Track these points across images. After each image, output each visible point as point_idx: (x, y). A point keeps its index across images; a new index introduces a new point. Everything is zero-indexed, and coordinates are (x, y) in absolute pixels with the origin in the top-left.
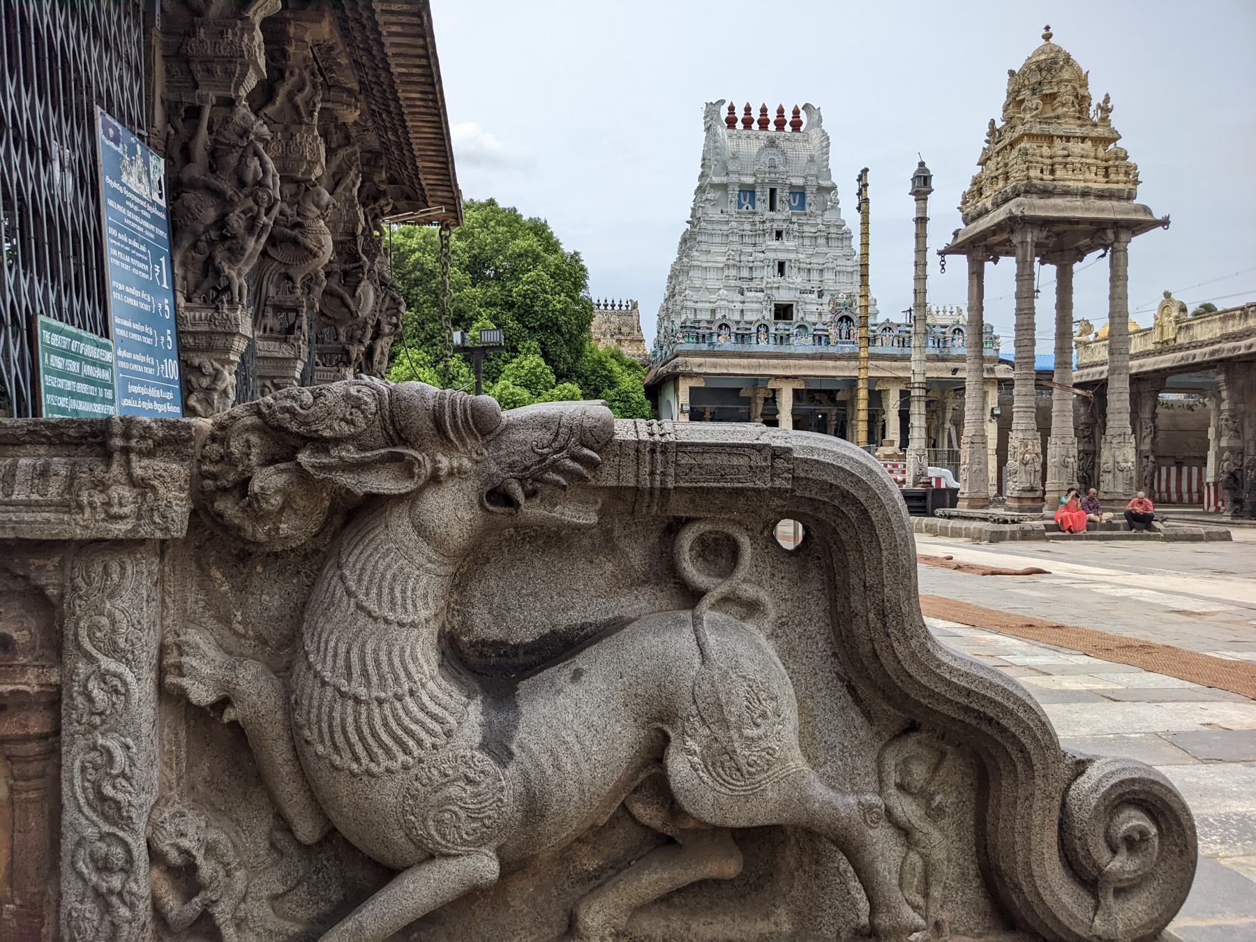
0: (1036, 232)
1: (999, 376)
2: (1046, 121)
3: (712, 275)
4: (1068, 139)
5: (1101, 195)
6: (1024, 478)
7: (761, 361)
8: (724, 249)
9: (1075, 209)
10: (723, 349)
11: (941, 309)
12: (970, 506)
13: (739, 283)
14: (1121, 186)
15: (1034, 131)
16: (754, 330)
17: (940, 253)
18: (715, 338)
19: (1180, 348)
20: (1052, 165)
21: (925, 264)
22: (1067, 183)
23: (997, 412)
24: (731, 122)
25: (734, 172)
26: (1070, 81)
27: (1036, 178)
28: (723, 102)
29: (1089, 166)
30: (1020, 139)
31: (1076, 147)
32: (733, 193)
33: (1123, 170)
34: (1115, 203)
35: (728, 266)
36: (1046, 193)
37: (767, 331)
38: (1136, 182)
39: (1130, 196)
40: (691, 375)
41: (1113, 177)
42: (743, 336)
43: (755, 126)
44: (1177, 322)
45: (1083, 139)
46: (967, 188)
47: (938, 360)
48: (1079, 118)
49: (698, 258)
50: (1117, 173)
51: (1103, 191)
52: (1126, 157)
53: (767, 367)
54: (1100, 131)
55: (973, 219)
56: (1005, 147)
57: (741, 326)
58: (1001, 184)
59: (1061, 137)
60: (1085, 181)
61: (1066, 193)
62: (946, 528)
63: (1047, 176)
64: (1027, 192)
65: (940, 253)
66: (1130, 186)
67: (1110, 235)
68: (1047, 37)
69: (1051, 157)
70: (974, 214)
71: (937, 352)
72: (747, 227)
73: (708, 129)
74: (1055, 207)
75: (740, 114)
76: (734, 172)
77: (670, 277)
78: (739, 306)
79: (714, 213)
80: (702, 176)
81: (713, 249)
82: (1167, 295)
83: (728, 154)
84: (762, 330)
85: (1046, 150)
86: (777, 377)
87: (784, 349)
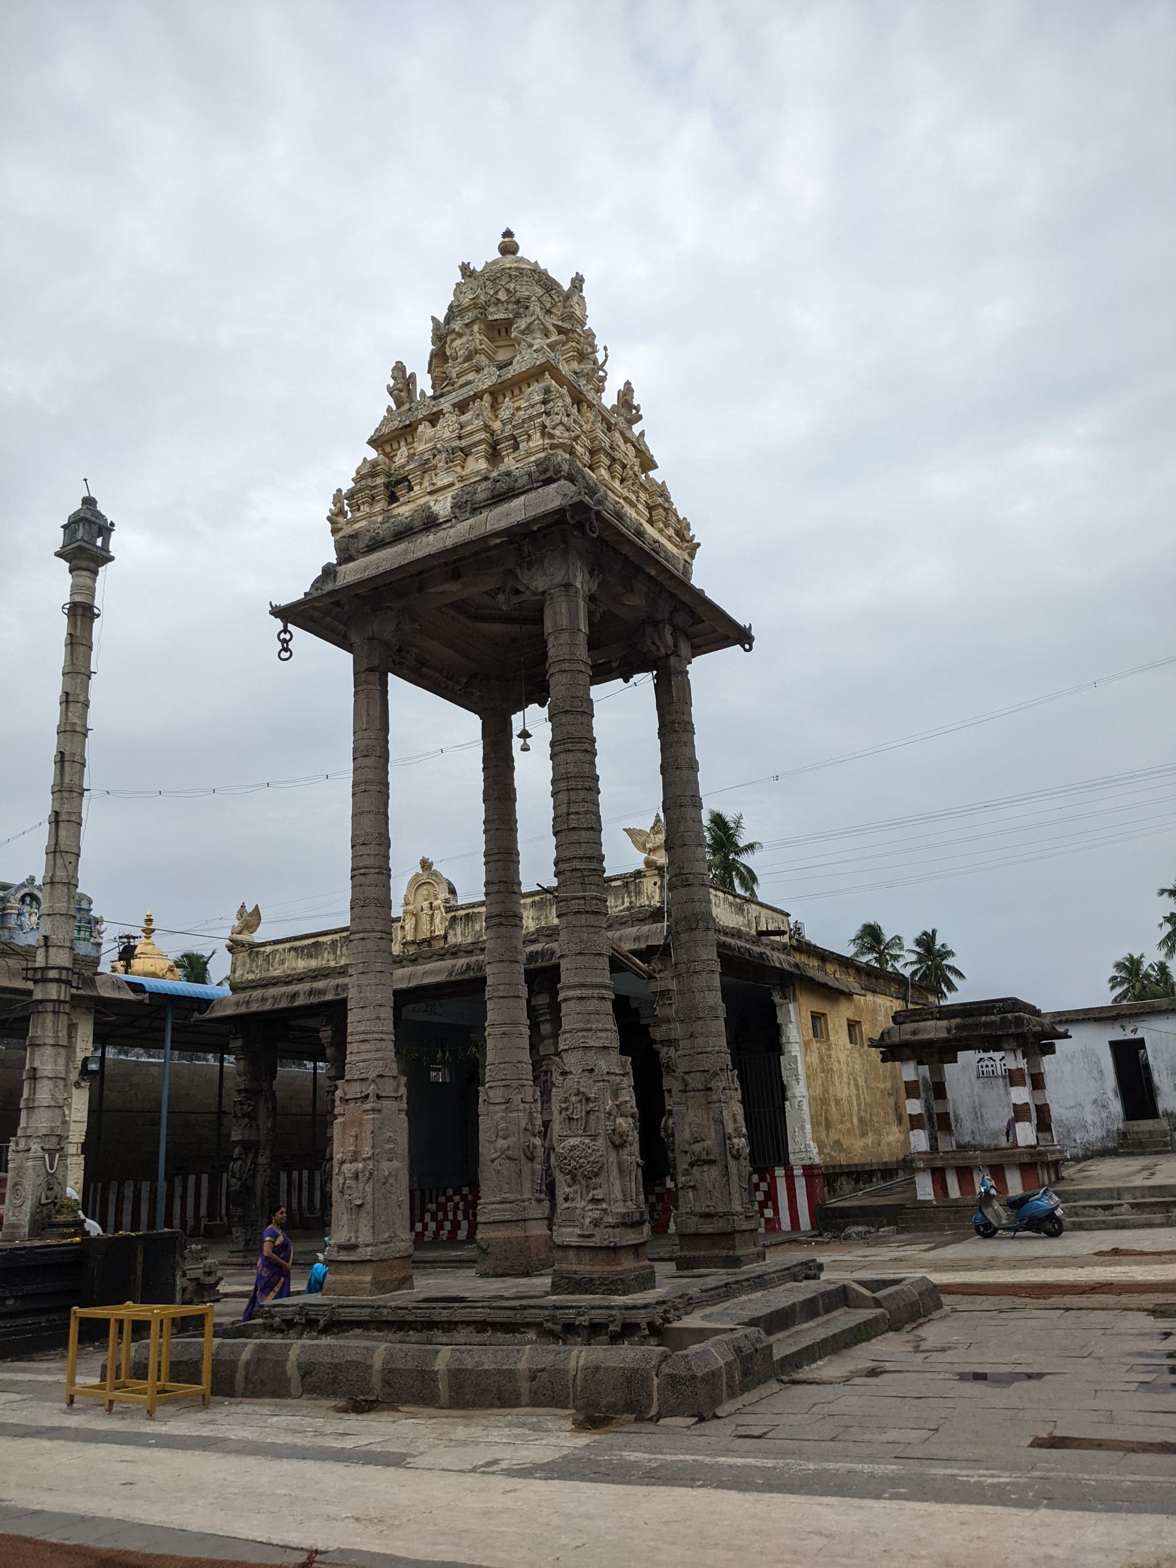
0: (587, 577)
6: (617, 1193)
12: (380, 1286)
17: (277, 612)
19: (455, 952)
21: (86, 705)
23: (93, 1067)
30: (535, 374)
44: (448, 910)
46: (347, 485)
55: (376, 545)
56: (478, 396)
58: (478, 464)
62: (426, 1377)
65: (277, 612)
70: (384, 531)
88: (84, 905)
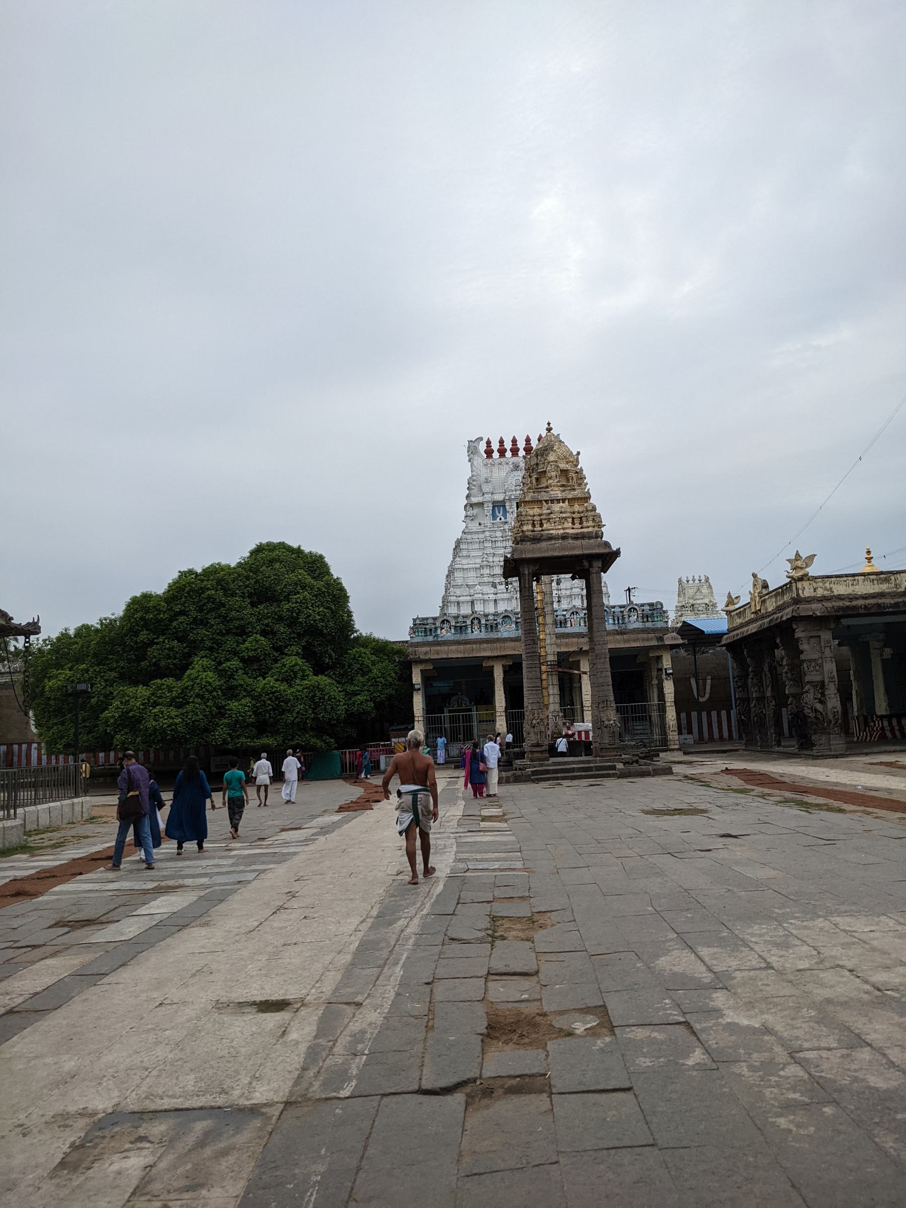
1: (666, 643)
2: (538, 490)
3: (472, 574)
4: (552, 501)
5: (576, 537)
7: (474, 646)
8: (480, 553)
9: (554, 550)
10: (444, 639)
11: (690, 579)
13: (491, 580)
14: (590, 529)
15: (527, 499)
16: (469, 622)
18: (439, 631)
20: (541, 520)
22: (551, 532)
24: (489, 453)
25: (487, 493)
26: (556, 462)
27: (528, 531)
28: (481, 439)
29: (566, 518)
31: (556, 507)
32: (489, 508)
33: (591, 518)
34: (585, 542)
35: (482, 567)
36: (536, 540)
37: (480, 622)
38: (600, 526)
39: (599, 535)
40: (420, 662)
41: (585, 524)
42: (461, 627)
43: (508, 454)
45: (564, 501)
47: (618, 634)
48: (563, 486)
49: (464, 562)
50: (587, 521)
51: (577, 534)
52: (594, 509)
53: (479, 651)
54: (577, 493)
57: (460, 619)
59: (546, 501)
60: (563, 529)
61: (550, 538)
63: (538, 528)
64: (522, 541)
66: (596, 529)
67: (586, 564)
68: (549, 430)
69: (540, 515)
71: (617, 628)
72: (499, 534)
73: (470, 461)
74: (540, 550)
75: (495, 446)
76: (487, 493)
77: (447, 576)
78: (492, 597)
79: (474, 526)
80: (468, 497)
81: (473, 554)
82: (755, 576)
83: (482, 479)
84: (476, 622)
85: (536, 511)
86: (489, 658)
87: (493, 635)
88: (659, 606)
